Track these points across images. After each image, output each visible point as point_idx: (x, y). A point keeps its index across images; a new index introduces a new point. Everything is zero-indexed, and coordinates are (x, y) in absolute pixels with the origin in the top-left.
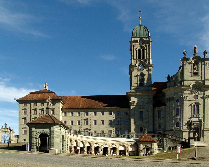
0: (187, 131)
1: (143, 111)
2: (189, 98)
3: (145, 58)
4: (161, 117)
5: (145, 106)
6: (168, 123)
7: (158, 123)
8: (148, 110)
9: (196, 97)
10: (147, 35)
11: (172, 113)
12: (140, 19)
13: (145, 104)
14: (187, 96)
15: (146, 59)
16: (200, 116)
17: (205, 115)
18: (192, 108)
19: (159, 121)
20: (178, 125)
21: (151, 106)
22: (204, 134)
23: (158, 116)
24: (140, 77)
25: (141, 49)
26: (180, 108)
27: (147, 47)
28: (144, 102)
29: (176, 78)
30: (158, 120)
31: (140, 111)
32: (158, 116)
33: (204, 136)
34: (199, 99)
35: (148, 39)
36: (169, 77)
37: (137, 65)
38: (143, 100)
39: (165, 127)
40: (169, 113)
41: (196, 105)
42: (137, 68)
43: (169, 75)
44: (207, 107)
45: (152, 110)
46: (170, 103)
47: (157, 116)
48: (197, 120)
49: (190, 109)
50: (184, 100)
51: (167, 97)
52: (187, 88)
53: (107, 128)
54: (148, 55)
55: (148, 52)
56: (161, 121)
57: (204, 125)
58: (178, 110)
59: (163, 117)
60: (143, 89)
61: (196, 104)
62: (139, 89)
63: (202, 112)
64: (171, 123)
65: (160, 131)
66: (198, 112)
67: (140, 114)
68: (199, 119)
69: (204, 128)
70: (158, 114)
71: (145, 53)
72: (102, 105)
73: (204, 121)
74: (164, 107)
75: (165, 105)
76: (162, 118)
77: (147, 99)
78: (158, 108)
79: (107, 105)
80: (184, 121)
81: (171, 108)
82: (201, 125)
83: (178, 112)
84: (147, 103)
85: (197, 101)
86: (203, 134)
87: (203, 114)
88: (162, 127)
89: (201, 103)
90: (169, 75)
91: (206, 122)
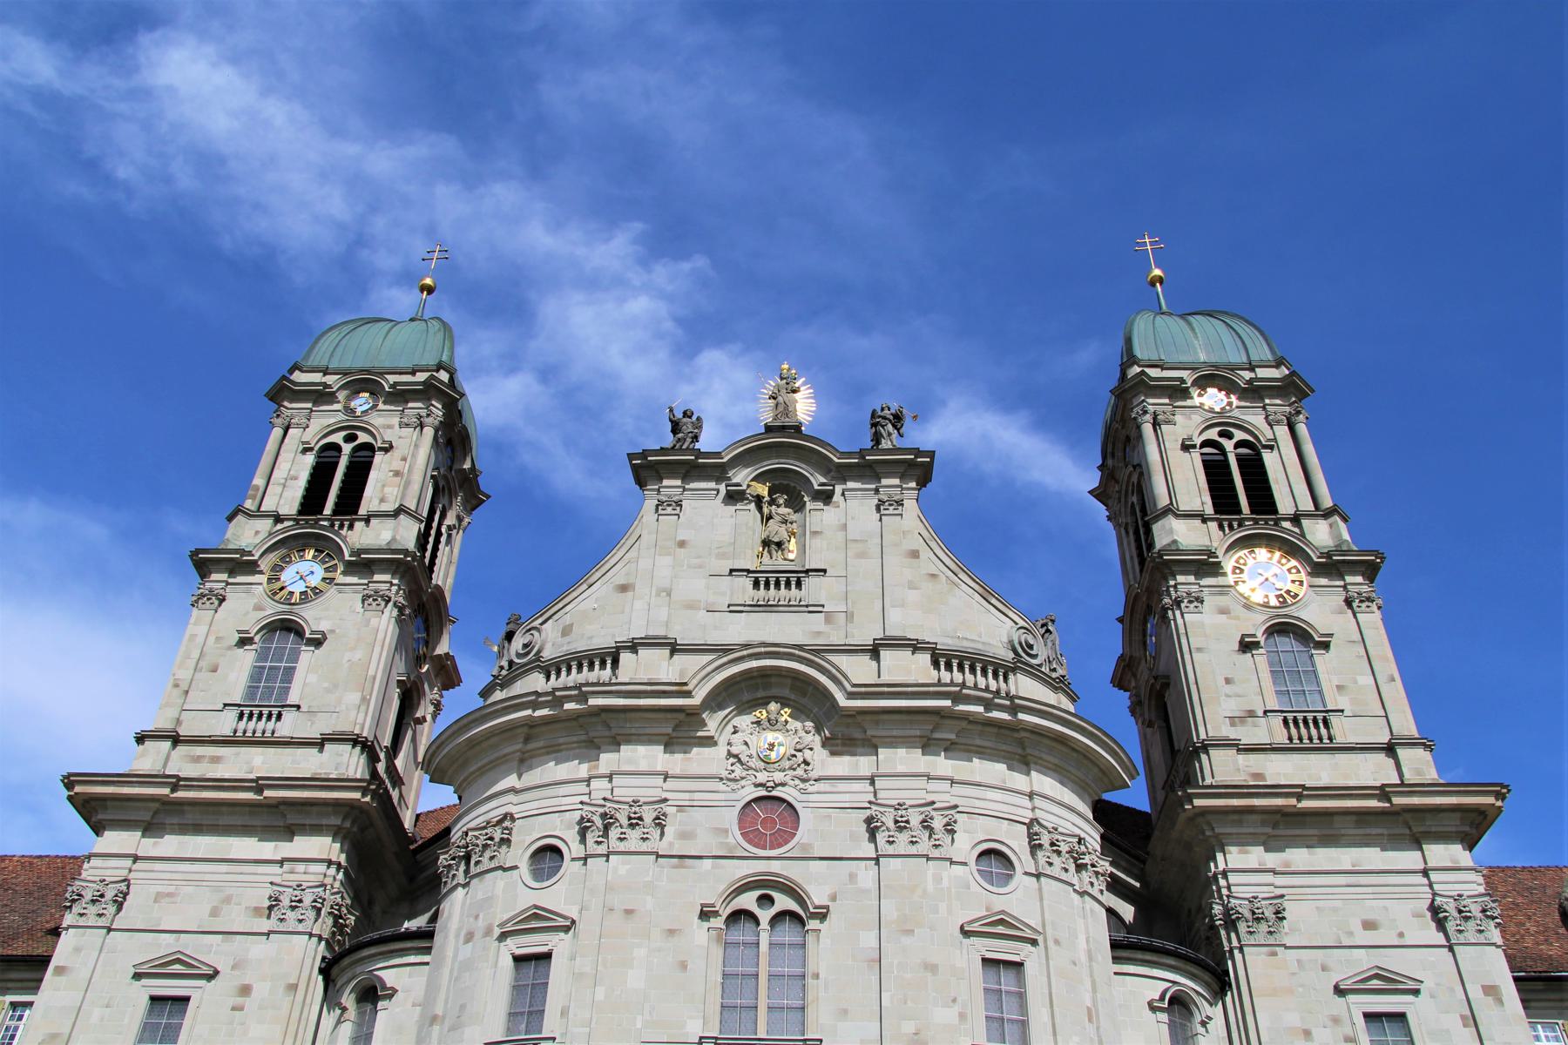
2: (684, 836)
13: (237, 919)
24: (262, 656)
25: (347, 448)
31: (153, 999)
44: (906, 940)
50: (622, 846)
71: (373, 475)
84: (257, 911)
85: (775, 867)
89: (828, 890)
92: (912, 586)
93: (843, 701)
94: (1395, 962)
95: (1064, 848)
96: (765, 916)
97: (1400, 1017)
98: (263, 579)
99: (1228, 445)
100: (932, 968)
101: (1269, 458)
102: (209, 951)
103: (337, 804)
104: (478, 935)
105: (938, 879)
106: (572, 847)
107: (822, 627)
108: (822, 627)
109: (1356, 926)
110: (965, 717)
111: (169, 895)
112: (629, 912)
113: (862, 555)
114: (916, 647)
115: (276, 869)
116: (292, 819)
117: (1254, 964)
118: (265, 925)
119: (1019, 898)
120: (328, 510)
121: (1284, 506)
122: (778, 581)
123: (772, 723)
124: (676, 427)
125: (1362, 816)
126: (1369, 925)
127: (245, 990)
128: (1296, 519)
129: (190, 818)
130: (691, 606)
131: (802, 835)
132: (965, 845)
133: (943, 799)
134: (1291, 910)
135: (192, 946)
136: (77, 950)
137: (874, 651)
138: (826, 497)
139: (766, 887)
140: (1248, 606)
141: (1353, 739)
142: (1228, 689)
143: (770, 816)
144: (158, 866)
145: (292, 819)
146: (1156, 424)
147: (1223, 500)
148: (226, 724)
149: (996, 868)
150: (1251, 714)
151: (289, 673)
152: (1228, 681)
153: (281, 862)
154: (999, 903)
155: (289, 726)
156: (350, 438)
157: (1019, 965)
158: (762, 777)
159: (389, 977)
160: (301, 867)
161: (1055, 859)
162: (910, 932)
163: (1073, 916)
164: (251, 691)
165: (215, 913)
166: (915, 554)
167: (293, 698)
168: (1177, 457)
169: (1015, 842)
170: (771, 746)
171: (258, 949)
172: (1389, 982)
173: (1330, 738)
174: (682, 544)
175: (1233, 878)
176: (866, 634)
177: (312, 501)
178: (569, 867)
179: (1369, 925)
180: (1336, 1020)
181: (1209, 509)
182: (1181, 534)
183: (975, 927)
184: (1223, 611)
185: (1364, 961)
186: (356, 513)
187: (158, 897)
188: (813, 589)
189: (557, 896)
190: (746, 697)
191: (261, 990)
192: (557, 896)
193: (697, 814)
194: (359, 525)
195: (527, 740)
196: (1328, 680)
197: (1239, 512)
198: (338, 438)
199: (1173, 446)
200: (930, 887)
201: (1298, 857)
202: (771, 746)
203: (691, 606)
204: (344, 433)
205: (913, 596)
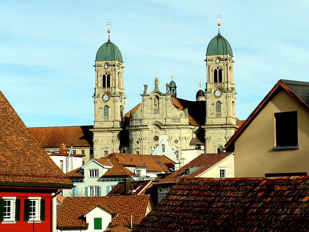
5: (109, 144)
28: (108, 140)
54: (114, 83)
60: (107, 124)
62: (103, 124)
71: (111, 80)
101: (223, 72)
107: (161, 116)
108: (161, 116)
111: (103, 140)
113: (164, 106)
120: (106, 87)
121: (223, 82)
122: (157, 111)
126: (219, 139)
130: (148, 114)
132: (173, 140)
136: (96, 147)
141: (223, 117)
147: (216, 81)
150: (212, 113)
155: (109, 120)
156: (106, 74)
164: (104, 115)
165: (108, 142)
166: (170, 106)
169: (178, 139)
174: (146, 105)
179: (219, 139)
180: (214, 149)
184: (212, 99)
187: (102, 140)
188: (161, 111)
189: (139, 146)
192: (139, 146)
194: (111, 89)
196: (222, 108)
203: (148, 114)
204: (105, 73)
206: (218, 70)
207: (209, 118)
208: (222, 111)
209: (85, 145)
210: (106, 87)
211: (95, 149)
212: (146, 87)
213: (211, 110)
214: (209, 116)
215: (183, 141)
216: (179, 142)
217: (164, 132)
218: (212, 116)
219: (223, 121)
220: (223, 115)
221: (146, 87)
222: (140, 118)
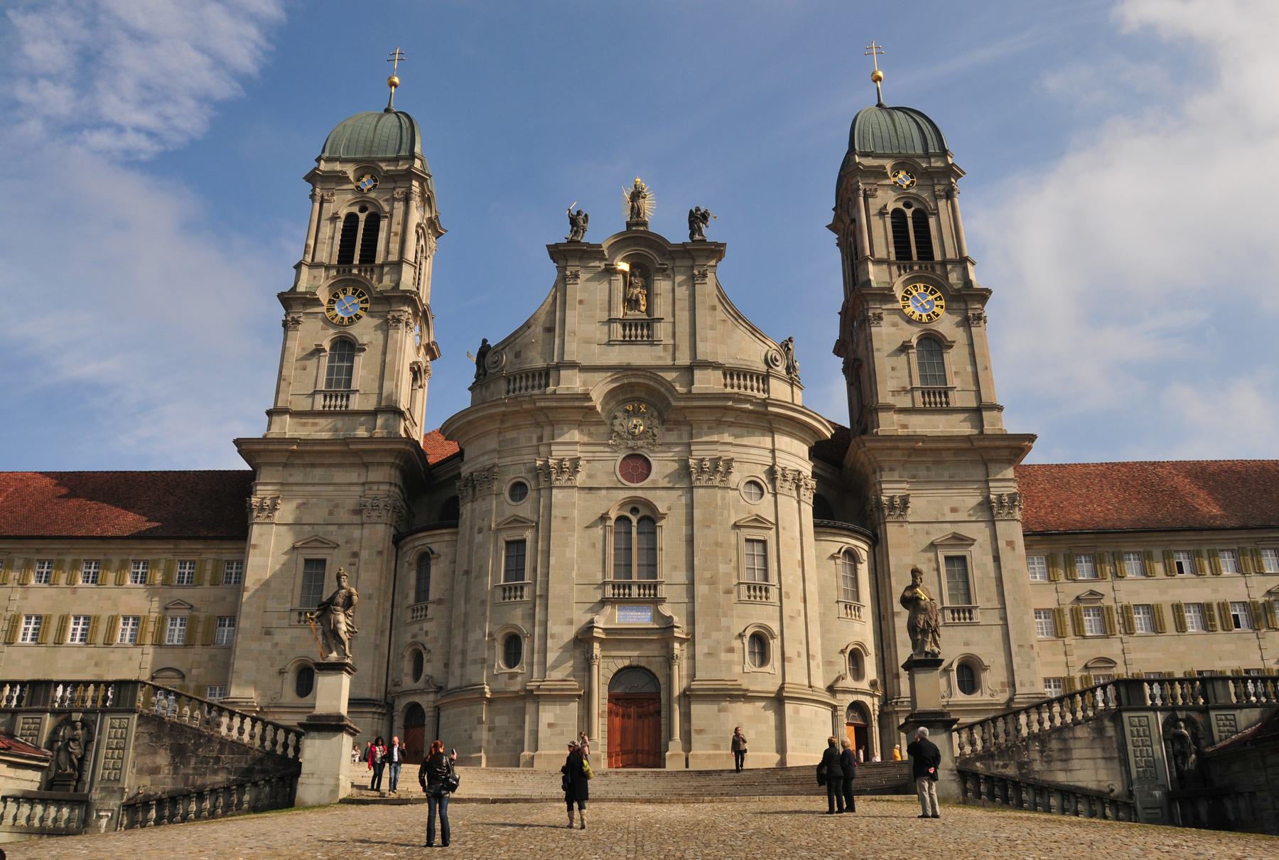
0: (570, 698)
1: (322, 562)
2: (590, 476)
3: (379, 259)
4: (431, 597)
5: (340, 525)
6: (457, 642)
7: (408, 638)
8: (355, 555)
9: (637, 466)
10: (406, 146)
11: (482, 574)
12: (393, 84)
14: (575, 462)
15: (382, 266)
16: (663, 591)
17: (701, 589)
18: (611, 539)
19: (415, 628)
20: (513, 648)
21: (379, 533)
22: (696, 723)
23: (417, 593)
24: (331, 360)
26: (528, 535)
27: (399, 207)
28: (337, 506)
29: (518, 355)
30: (409, 620)
31: (306, 561)
32: (412, 595)
33: (694, 736)
34: (654, 481)
35: (403, 166)
36: (484, 351)
37: (323, 296)
38: (331, 488)
39: (446, 665)
40: (467, 572)
41: (634, 520)
42: (323, 309)
43: (485, 341)
45: (380, 553)
46: (476, 505)
47: (407, 596)
48: (640, 618)
49: (594, 545)
50: (557, 483)
51: (465, 470)
52: (579, 411)
53: (96, 665)
54: (395, 247)
55: (397, 228)
56: (426, 626)
57: (692, 657)
58: (516, 548)
59: (439, 602)
61: (634, 511)
63: (675, 568)
64: (474, 636)
65: (417, 699)
66: (651, 567)
67: (307, 576)
68: (658, 616)
69: (692, 676)
70: (418, 580)
71: (382, 236)
72: (131, 521)
73: (691, 621)
74: (445, 535)
75: (449, 517)
76: (431, 607)
77: (353, 488)
78: (417, 543)
79: (145, 525)
80: (553, 628)
81: (479, 538)
82: (669, 659)
83: (515, 568)
84: (358, 512)
85: (639, 493)
86: (686, 717)
87: (681, 577)
88: (428, 669)
89: (666, 504)
90: (485, 341)
91: (706, 636)
92: (712, 328)
93: (674, 403)
94: (964, 530)
95: (790, 477)
96: (634, 520)
97: (963, 559)
98: (323, 309)
99: (909, 212)
100: (717, 544)
101: (932, 221)
102: (333, 533)
103: (391, 451)
104: (485, 530)
105: (723, 498)
106: (531, 485)
107: (662, 354)
108: (662, 354)
109: (947, 509)
110: (741, 410)
112: (564, 518)
114: (715, 366)
115: (360, 489)
116: (366, 459)
117: (893, 532)
118: (357, 519)
119: (764, 507)
120: (356, 262)
121: (938, 256)
123: (636, 413)
124: (573, 221)
125: (957, 451)
126: (954, 510)
127: (355, 555)
128: (944, 263)
129: (308, 460)
130: (588, 341)
131: (652, 476)
133: (726, 456)
134: (913, 502)
135: (321, 531)
136: (261, 535)
137: (690, 369)
138: (663, 271)
139: (635, 505)
140: (909, 321)
141: (958, 405)
142: (892, 374)
143: (637, 466)
144: (295, 488)
145: (366, 459)
146: (866, 198)
148: (319, 403)
149: (754, 490)
151: (350, 371)
152: (893, 369)
153: (364, 484)
154: (755, 510)
155: (356, 403)
156: (363, 210)
157: (764, 542)
158: (630, 443)
159: (435, 547)
160: (375, 487)
161: (787, 485)
162: (709, 527)
163: (796, 513)
165: (331, 513)
167: (355, 385)
168: (876, 222)
170: (636, 426)
171: (357, 533)
172: (959, 540)
173: (947, 403)
174: (581, 302)
175: (884, 486)
176: (684, 359)
177: (345, 254)
178: (531, 494)
179: (954, 510)
181: (893, 257)
182: (876, 275)
183: (741, 523)
184: (895, 325)
185: (949, 529)
186: (373, 261)
189: (525, 509)
190: (621, 397)
191: (364, 555)
193: (597, 464)
194: (377, 271)
195: (502, 422)
197: (910, 258)
198: (355, 209)
199: (873, 211)
200: (719, 502)
201: (922, 473)
202: (636, 426)
203: (588, 341)
205: (710, 334)
206: (909, 212)
207: (889, 408)
208: (953, 381)
209: (204, 533)
210: (356, 262)
211: (255, 546)
212: (577, 222)
213: (896, 373)
214: (890, 400)
215: (785, 491)
216: (768, 497)
217: (680, 437)
218: (905, 402)
219: (959, 426)
220: (957, 400)
221: (577, 222)
222: (540, 363)
